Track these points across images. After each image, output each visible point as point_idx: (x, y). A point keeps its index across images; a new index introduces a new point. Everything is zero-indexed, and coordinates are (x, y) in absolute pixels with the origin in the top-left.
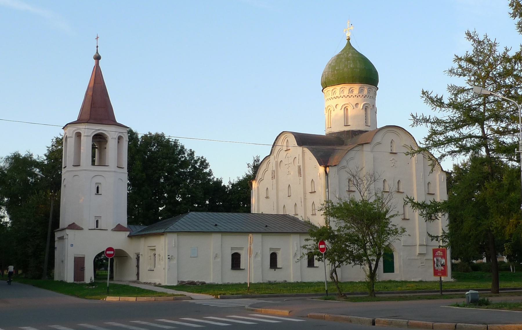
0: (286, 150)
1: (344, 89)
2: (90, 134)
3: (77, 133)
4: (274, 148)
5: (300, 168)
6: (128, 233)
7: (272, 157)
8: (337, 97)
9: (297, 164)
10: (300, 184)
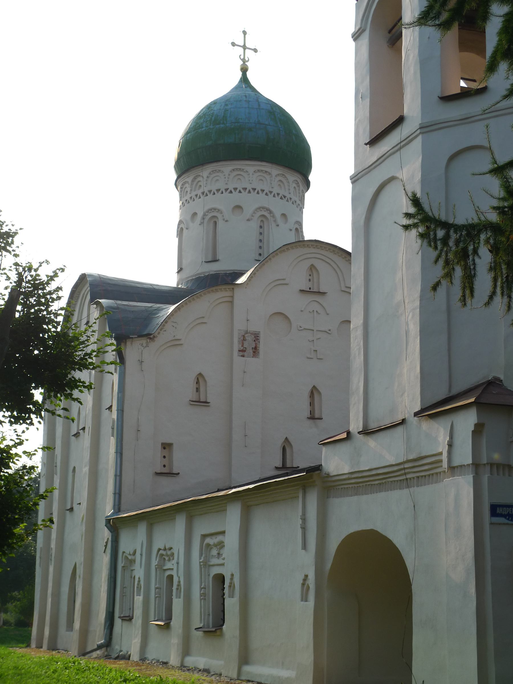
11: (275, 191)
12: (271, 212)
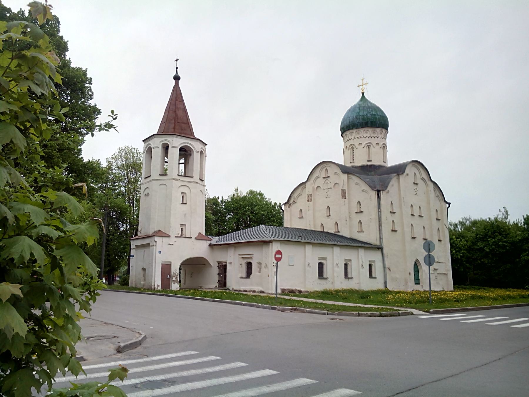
0: (324, 177)
1: (368, 131)
2: (176, 146)
3: (163, 144)
5: (345, 191)
6: (209, 242)
8: (360, 137)
10: (344, 205)
11: (356, 137)
12: (354, 145)
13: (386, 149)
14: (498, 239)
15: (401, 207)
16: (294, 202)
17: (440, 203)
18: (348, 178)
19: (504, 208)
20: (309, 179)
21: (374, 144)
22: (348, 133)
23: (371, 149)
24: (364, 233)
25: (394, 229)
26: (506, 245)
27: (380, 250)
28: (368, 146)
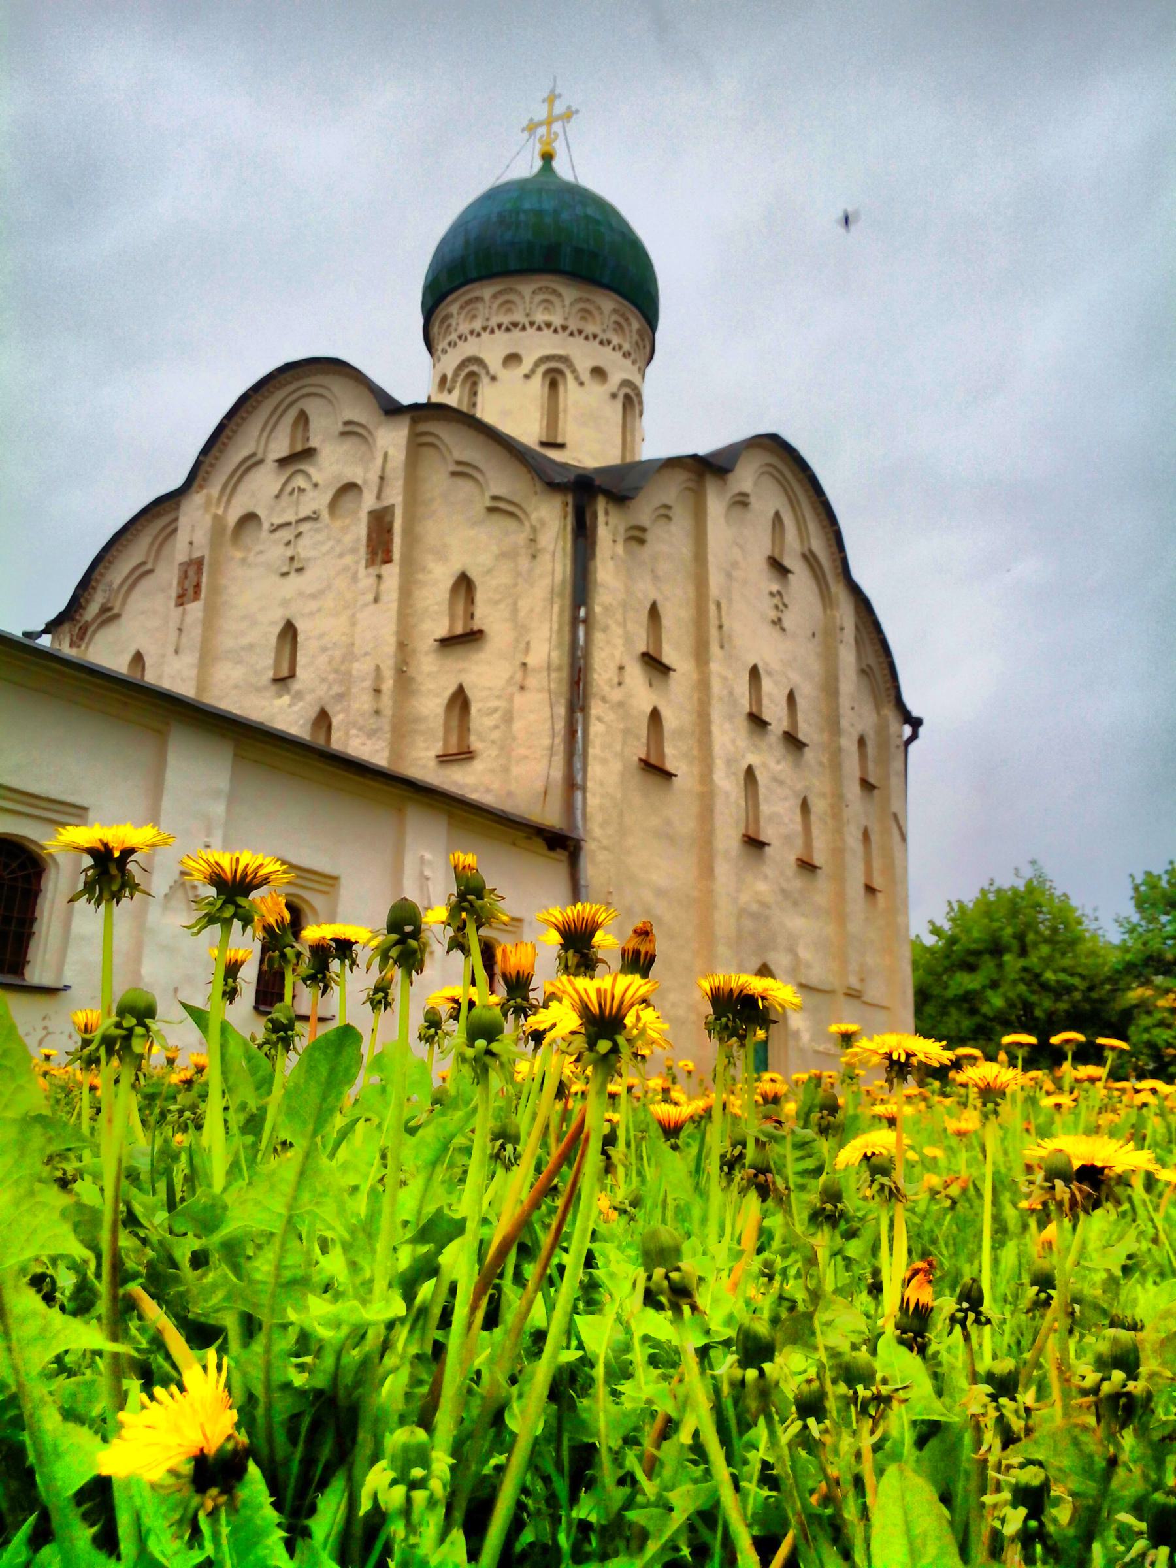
1: (552, 298)
4: (209, 459)
5: (388, 519)
7: (197, 499)
8: (515, 325)
9: (369, 501)
10: (376, 600)
11: (493, 323)
13: (637, 412)
14: (1041, 958)
15: (701, 655)
16: (109, 614)
17: (878, 713)
18: (417, 446)
19: (1033, 862)
20: (201, 474)
21: (583, 365)
22: (452, 307)
23: (566, 391)
24: (478, 765)
25: (653, 761)
26: (1073, 985)
27: (562, 855)
28: (552, 375)
